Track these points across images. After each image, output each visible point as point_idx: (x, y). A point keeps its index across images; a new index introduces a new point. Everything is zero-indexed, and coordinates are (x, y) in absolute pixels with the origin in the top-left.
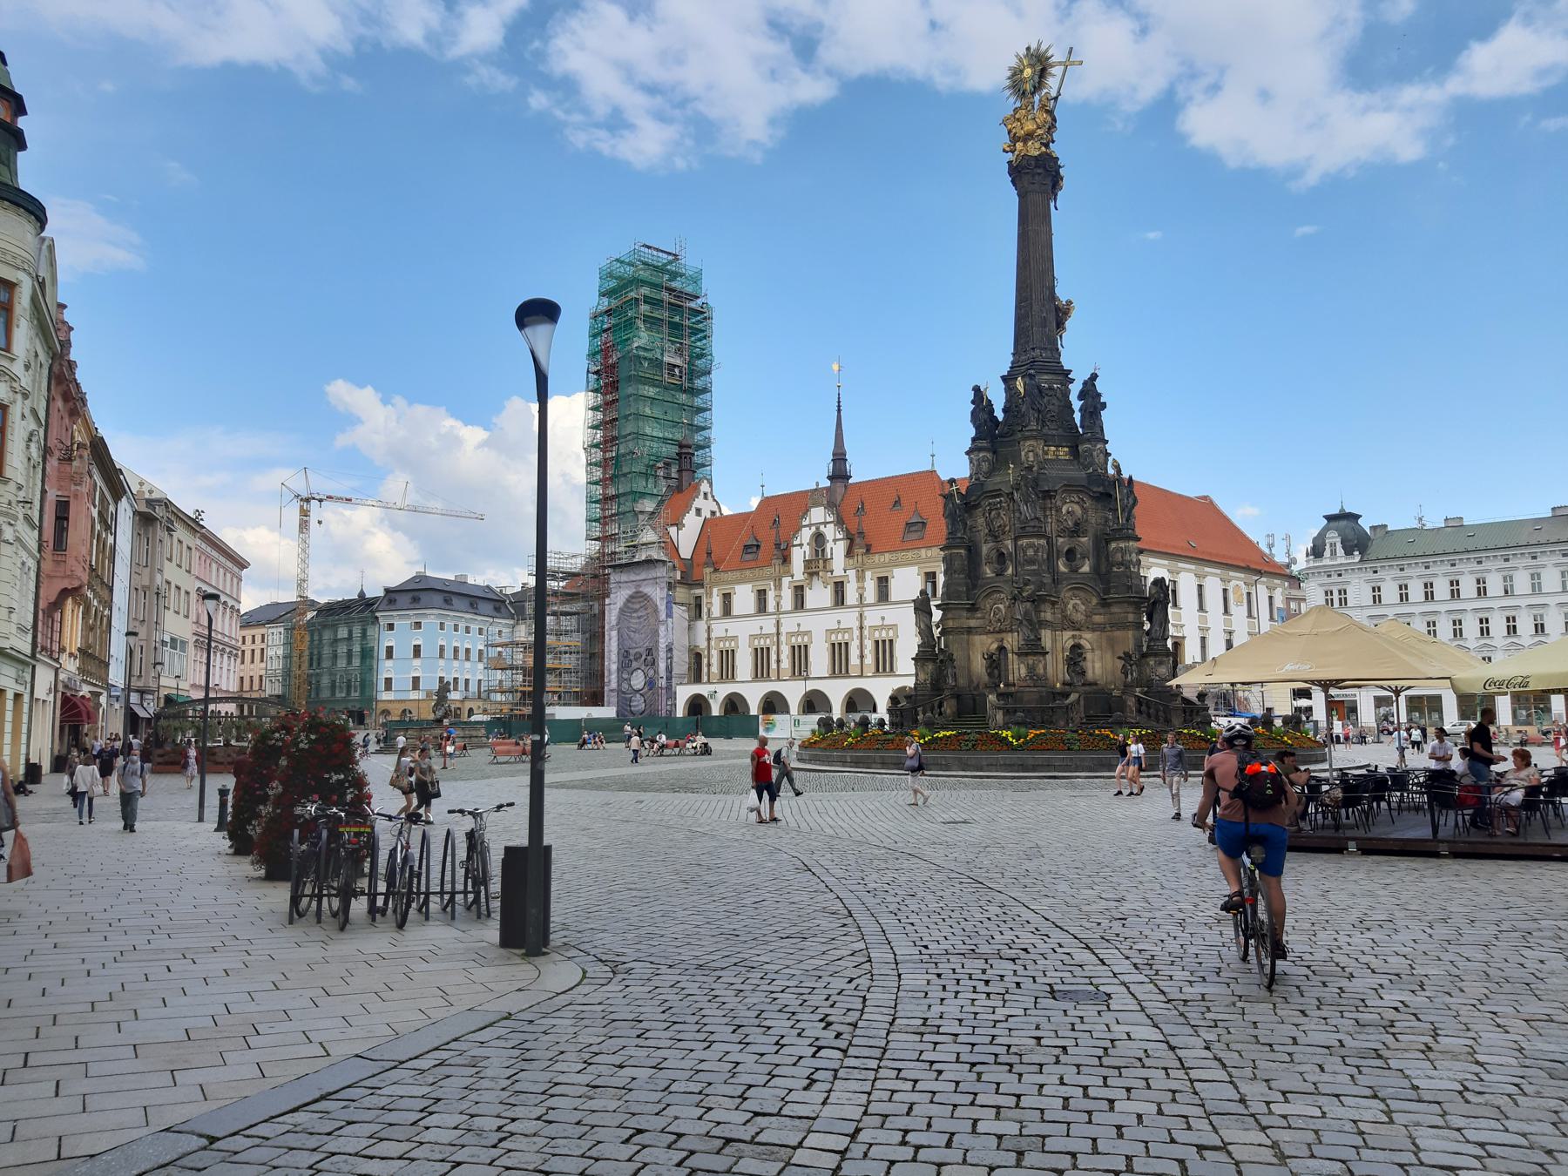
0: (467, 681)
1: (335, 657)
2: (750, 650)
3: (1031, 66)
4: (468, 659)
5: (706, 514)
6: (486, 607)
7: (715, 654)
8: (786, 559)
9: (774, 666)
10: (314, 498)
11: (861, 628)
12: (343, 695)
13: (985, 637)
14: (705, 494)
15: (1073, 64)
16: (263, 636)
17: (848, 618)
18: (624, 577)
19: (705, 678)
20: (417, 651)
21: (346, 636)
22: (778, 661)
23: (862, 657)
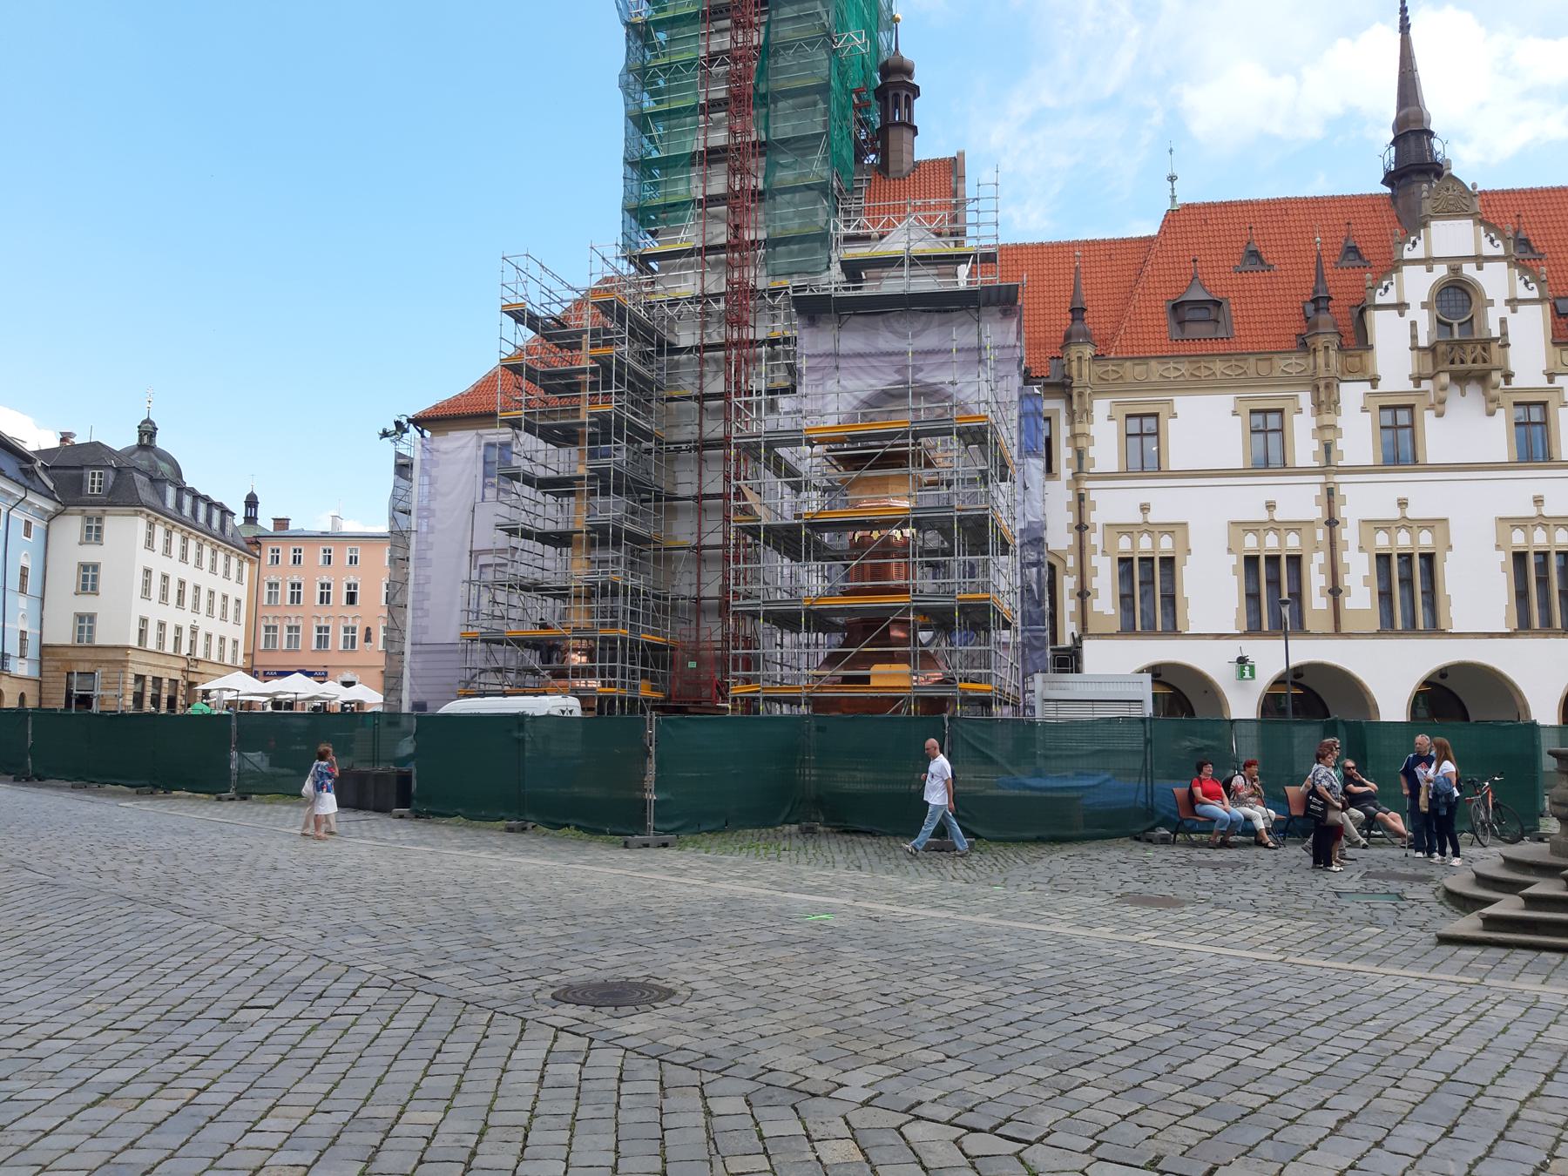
2: (1235, 560)
8: (1357, 339)
9: (1316, 601)
18: (852, 342)
22: (1335, 591)
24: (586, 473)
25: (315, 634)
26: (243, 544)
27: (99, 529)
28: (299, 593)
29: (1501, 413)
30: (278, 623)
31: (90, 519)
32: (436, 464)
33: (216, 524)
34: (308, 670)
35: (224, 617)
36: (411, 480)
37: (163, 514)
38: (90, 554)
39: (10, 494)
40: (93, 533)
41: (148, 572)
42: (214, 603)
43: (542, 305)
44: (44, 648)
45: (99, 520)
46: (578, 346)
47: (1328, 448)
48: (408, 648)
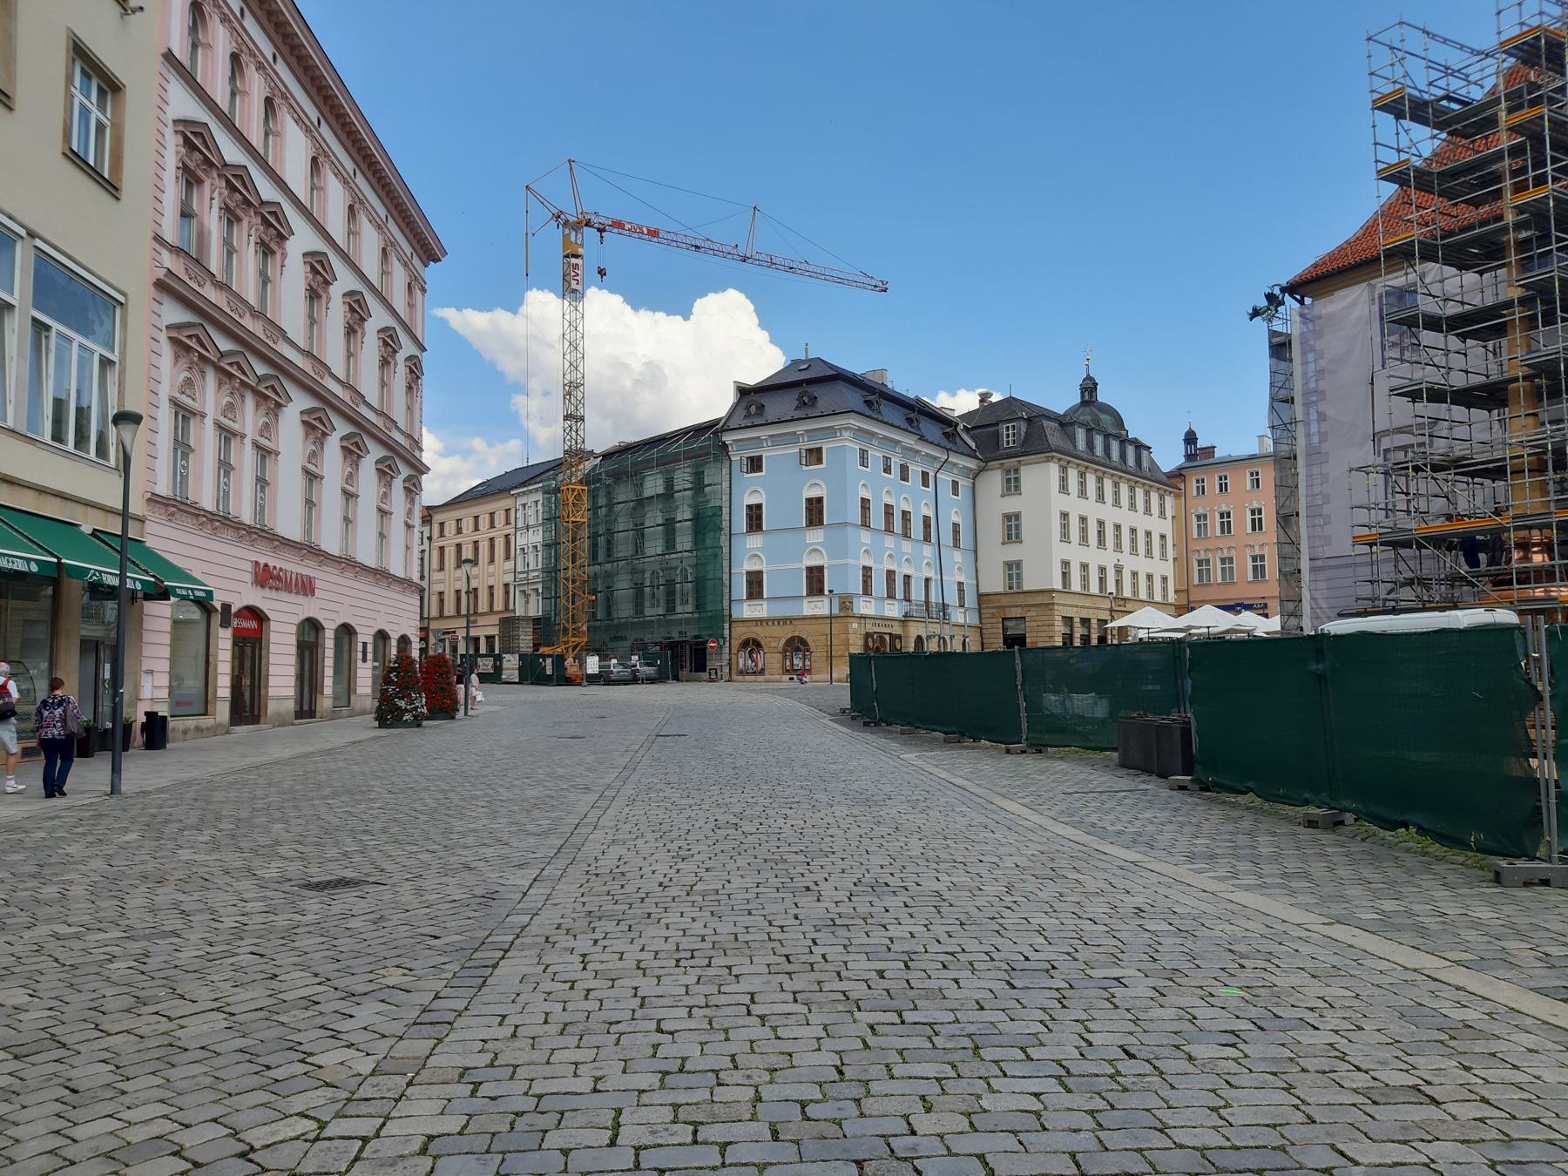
0: (907, 578)
1: (640, 533)
4: (906, 535)
6: (932, 430)
10: (588, 224)
12: (661, 611)
16: (507, 511)
20: (815, 512)
21: (660, 490)
24: (1515, 293)
25: (1250, 564)
26: (1165, 479)
27: (1017, 480)
28: (1229, 522)
30: (1210, 555)
31: (1008, 472)
32: (1319, 335)
33: (1131, 461)
34: (1246, 602)
35: (1149, 554)
36: (1291, 360)
37: (1073, 457)
38: (1012, 504)
39: (935, 458)
40: (1012, 485)
41: (1065, 515)
42: (1147, 544)
43: (1430, 84)
44: (981, 597)
45: (1017, 471)
46: (1492, 122)
48: (1305, 565)
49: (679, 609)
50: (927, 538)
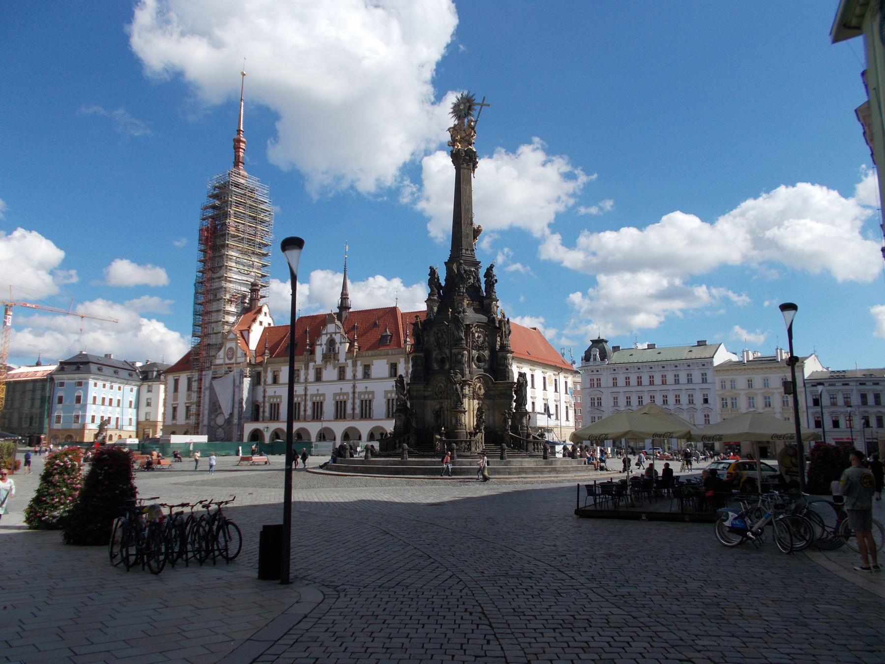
3: (465, 104)
5: (265, 325)
6: (125, 374)
7: (267, 405)
8: (312, 352)
9: (302, 413)
11: (354, 393)
13: (433, 401)
14: (265, 313)
15: (485, 105)
17: (347, 387)
19: (261, 419)
23: (354, 409)
29: (336, 369)
47: (306, 378)
49: (34, 425)
50: (118, 405)
